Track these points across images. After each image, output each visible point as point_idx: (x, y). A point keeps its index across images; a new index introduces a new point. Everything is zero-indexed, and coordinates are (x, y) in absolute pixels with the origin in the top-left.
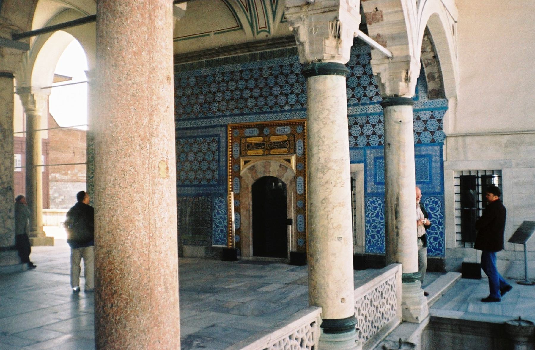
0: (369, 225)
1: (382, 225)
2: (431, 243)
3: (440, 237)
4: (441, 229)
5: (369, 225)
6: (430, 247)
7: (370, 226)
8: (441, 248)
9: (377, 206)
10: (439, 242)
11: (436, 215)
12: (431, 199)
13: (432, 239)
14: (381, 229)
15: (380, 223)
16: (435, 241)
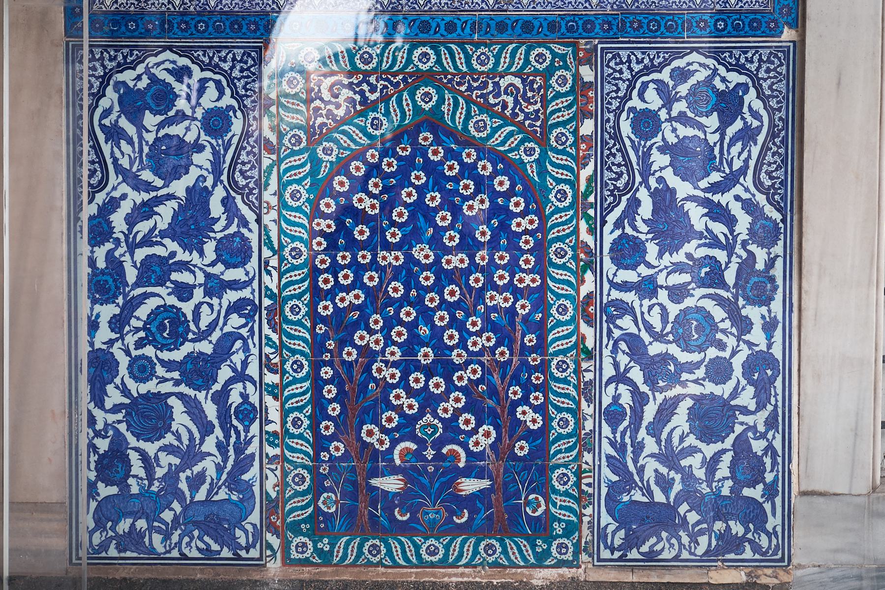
0: (107, 311)
1: (236, 307)
2: (669, 458)
3: (747, 399)
4: (757, 335)
5: (107, 311)
6: (665, 484)
7: (118, 323)
8: (755, 493)
9: (190, 132)
10: (741, 447)
11: (718, 213)
12: (682, 75)
13: (680, 420)
14: (223, 351)
15: (215, 287)
16: (708, 435)
